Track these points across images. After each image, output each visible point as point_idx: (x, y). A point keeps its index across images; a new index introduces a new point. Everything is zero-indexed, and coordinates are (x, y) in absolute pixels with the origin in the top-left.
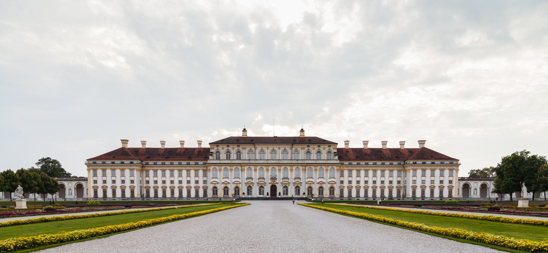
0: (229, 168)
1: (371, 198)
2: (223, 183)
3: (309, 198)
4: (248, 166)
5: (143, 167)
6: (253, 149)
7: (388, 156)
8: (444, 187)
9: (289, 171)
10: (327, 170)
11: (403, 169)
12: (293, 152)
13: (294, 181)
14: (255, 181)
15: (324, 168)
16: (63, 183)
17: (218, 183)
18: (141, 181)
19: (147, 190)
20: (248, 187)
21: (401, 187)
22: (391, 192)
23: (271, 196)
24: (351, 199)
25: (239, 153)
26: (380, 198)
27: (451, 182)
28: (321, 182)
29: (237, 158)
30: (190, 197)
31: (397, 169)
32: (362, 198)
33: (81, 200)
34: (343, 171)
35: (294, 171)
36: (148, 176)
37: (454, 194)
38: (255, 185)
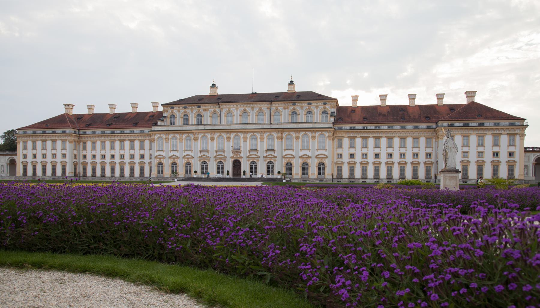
0: (178, 136)
1: (383, 180)
2: (170, 157)
4: (203, 134)
5: (79, 137)
6: (218, 110)
7: (414, 116)
8: (499, 162)
9: (259, 140)
10: (314, 138)
11: (435, 134)
12: (272, 113)
13: (265, 155)
14: (262, 153)
15: (310, 134)
16: (13, 157)
17: (164, 158)
18: (75, 155)
19: (84, 166)
20: (203, 163)
21: (432, 163)
22: (390, 171)
23: (233, 175)
24: (353, 181)
25: (199, 115)
26: (398, 180)
27: (511, 154)
28: (305, 156)
30: (134, 177)
31: (426, 135)
32: (371, 180)
33: (13, 178)
34: (342, 139)
35: (265, 140)
36: (85, 148)
37: (518, 174)
38: (212, 159)
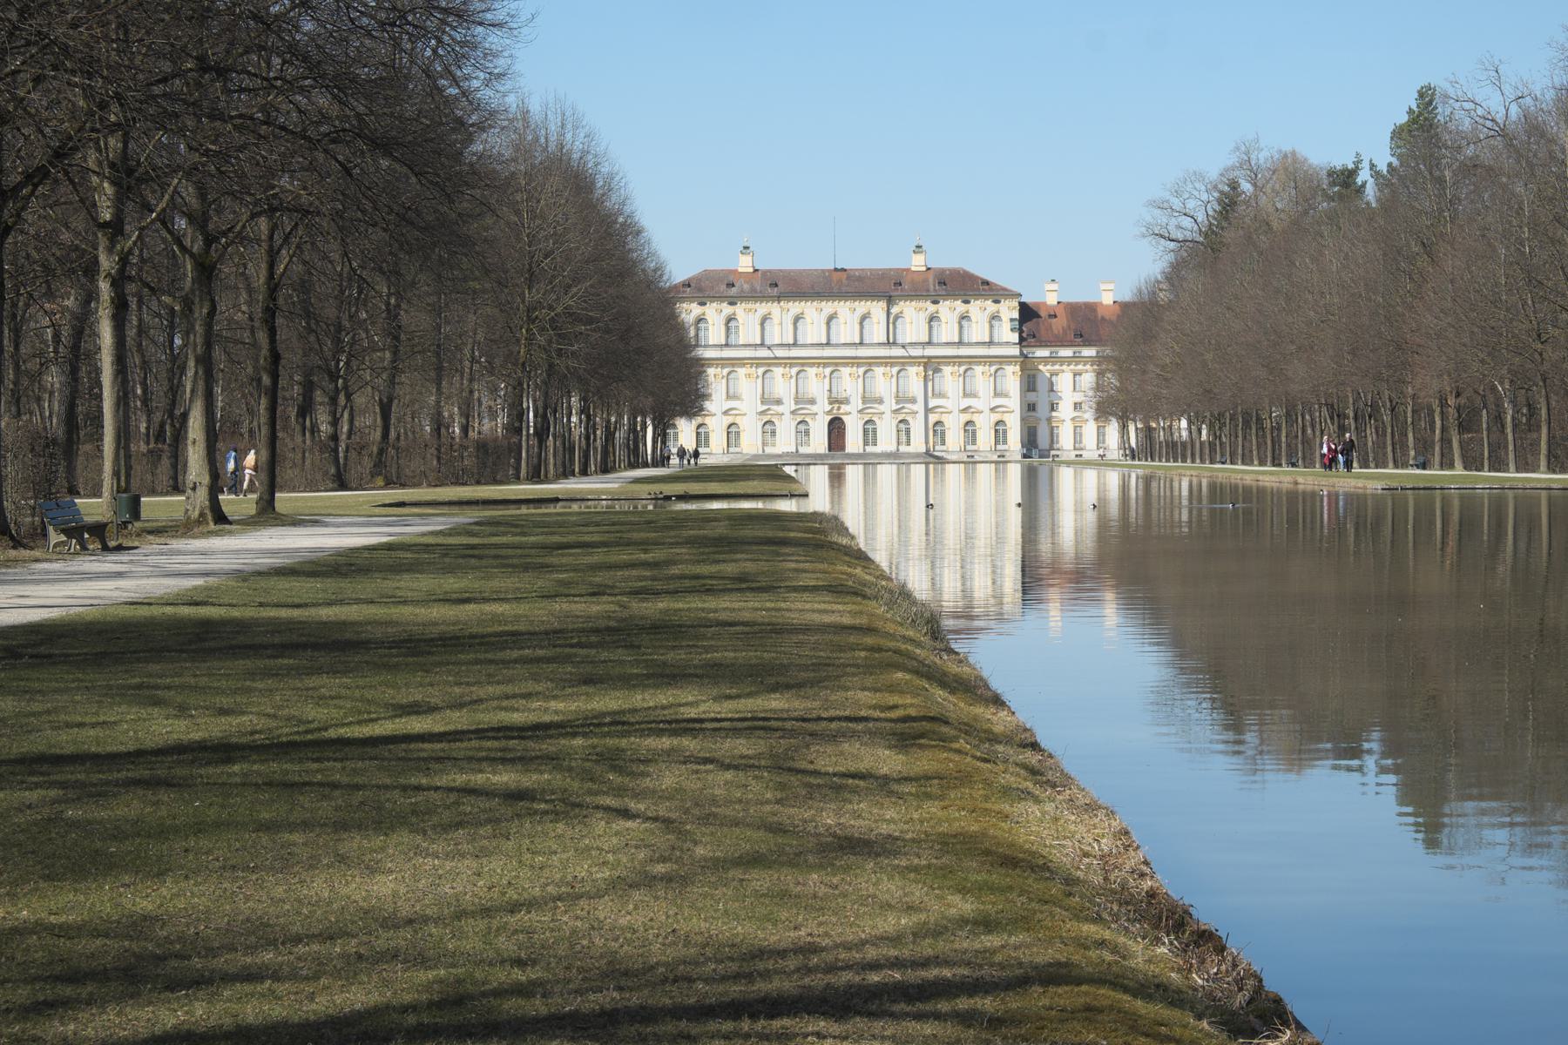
3: (936, 454)
13: (895, 407)
29: (727, 337)
